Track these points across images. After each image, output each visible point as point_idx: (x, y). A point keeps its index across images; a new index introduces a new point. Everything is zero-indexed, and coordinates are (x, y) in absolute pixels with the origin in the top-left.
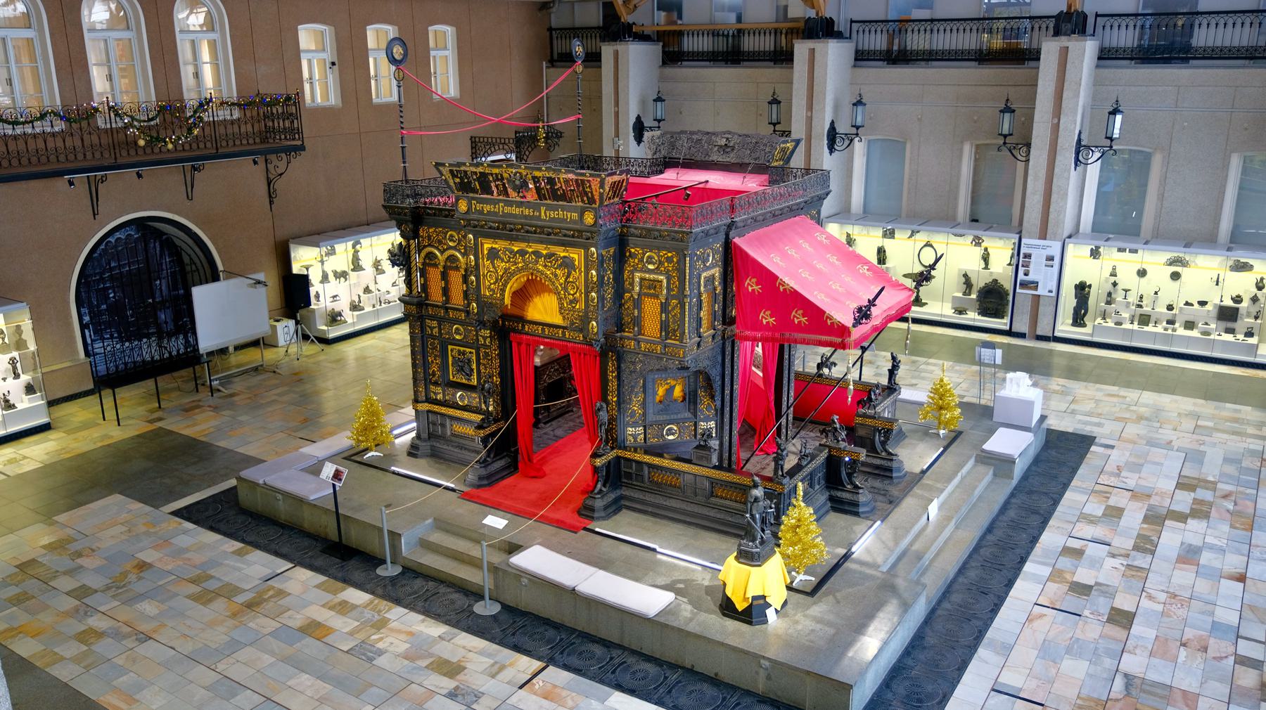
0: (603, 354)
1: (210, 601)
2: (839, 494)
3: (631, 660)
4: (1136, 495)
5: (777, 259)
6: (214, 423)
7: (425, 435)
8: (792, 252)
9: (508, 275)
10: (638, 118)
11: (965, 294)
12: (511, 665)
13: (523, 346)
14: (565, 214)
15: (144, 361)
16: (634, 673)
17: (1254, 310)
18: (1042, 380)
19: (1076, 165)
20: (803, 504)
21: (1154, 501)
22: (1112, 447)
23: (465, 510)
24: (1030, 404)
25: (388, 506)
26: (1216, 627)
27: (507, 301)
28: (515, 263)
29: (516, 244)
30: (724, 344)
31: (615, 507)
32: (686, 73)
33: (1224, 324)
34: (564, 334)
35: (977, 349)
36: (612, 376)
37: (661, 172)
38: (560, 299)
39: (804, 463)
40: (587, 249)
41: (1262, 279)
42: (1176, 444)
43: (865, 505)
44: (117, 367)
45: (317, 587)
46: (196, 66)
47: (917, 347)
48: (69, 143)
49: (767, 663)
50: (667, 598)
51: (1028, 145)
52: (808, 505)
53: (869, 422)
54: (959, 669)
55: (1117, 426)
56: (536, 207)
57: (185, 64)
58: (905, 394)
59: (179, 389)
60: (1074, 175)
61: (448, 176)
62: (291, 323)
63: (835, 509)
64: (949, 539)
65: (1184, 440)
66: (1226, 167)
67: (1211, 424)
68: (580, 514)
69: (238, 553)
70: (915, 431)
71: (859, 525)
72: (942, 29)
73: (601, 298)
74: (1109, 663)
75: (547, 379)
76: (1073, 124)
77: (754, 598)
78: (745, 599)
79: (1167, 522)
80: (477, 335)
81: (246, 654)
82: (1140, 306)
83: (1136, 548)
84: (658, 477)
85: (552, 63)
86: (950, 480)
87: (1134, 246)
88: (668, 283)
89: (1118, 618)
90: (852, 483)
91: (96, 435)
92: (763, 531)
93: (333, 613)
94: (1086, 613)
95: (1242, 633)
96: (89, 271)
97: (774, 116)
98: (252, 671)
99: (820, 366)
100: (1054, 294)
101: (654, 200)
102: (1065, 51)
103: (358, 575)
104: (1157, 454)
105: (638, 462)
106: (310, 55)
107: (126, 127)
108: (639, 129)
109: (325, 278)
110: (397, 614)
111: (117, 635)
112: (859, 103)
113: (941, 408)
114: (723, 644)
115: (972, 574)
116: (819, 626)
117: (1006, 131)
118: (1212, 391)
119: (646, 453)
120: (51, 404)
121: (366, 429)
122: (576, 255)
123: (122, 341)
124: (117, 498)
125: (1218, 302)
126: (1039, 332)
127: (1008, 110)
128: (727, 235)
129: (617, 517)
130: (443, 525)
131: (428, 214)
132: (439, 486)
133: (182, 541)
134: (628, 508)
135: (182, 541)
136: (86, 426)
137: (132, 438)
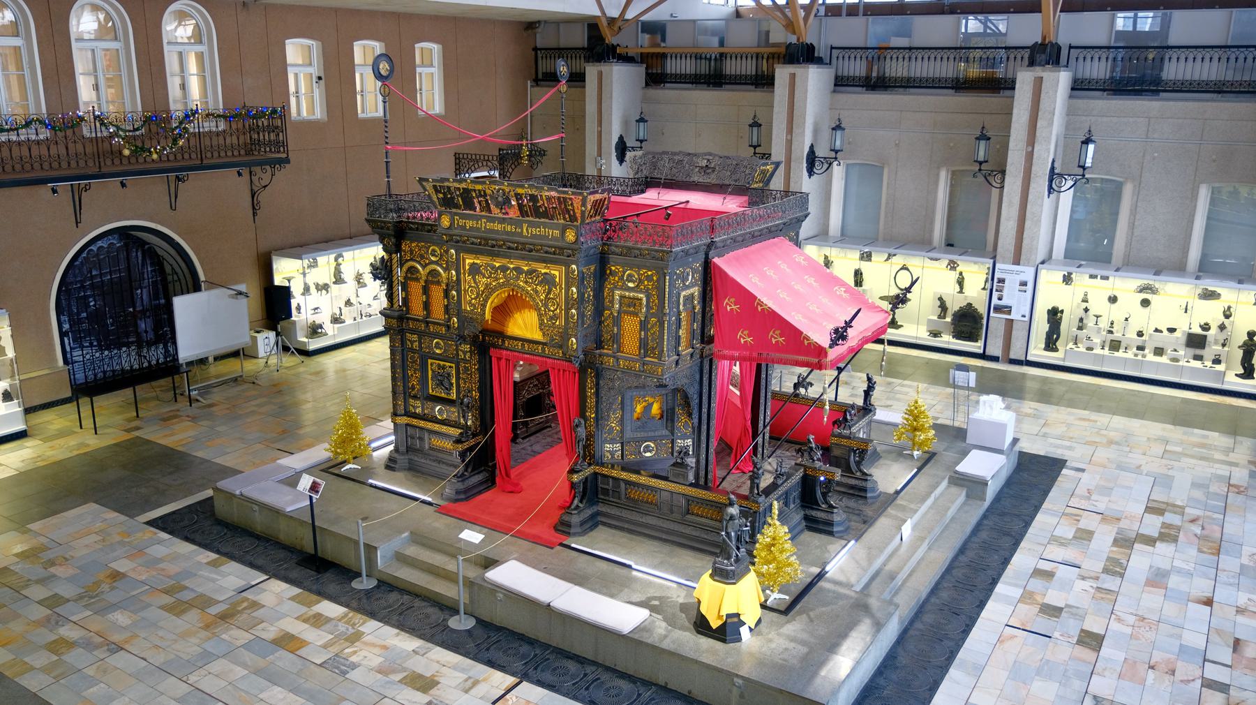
0: (583, 370)
1: (183, 612)
2: (814, 513)
3: (605, 677)
4: (1105, 518)
5: (755, 280)
6: (192, 433)
7: (403, 449)
8: (770, 273)
9: (489, 290)
10: (621, 138)
11: (940, 317)
12: (484, 680)
13: (503, 362)
14: (547, 232)
15: (122, 370)
16: (608, 690)
17: (1221, 338)
18: (1015, 403)
19: (1049, 193)
20: (778, 523)
21: (1124, 524)
22: (1083, 470)
23: (441, 523)
24: (1002, 427)
25: (364, 519)
26: (1183, 650)
27: (488, 316)
28: (497, 279)
29: (498, 259)
30: (702, 363)
31: (592, 523)
32: (667, 93)
33: (1192, 351)
34: (543, 350)
35: (952, 371)
36: (590, 392)
37: (643, 192)
38: (540, 315)
39: (780, 482)
40: (568, 266)
41: (1229, 308)
42: (1145, 469)
43: (840, 524)
44: (95, 375)
45: (292, 599)
46: (183, 78)
47: (892, 369)
48: (53, 151)
49: (741, 682)
50: (643, 614)
51: (1003, 172)
52: (783, 524)
53: (844, 442)
54: (964, 631)
55: (1089, 450)
56: (518, 224)
57: (172, 75)
58: (880, 415)
59: (157, 398)
60: (1047, 202)
61: (432, 191)
62: (272, 335)
63: (810, 529)
64: (922, 559)
65: (1156, 466)
66: (1194, 197)
67: (1179, 449)
68: (555, 528)
69: (213, 564)
70: (890, 452)
71: (834, 545)
72: (920, 57)
73: (581, 315)
74: (1078, 685)
75: (526, 395)
76: (1047, 153)
77: (728, 616)
78: (720, 617)
79: (1136, 546)
80: (457, 350)
81: (217, 666)
82: (1111, 332)
83: (1106, 571)
84: (635, 494)
85: (537, 81)
86: (924, 500)
87: (1105, 273)
89: (1087, 640)
90: (827, 502)
91: (72, 443)
92: (738, 549)
93: (307, 626)
94: (1056, 635)
95: (1209, 656)
96: (70, 279)
97: (755, 139)
98: (224, 684)
99: (796, 386)
100: (1027, 319)
101: (636, 219)
102: (1039, 82)
103: (332, 588)
104: (1127, 478)
105: (613, 478)
106: (296, 70)
107: (111, 136)
108: (622, 149)
109: (307, 290)
110: (372, 629)
111: (89, 646)
112: (838, 127)
113: (915, 429)
114: (697, 662)
115: (944, 595)
116: (792, 645)
117: (981, 158)
118: (1182, 417)
119: (623, 469)
120: (28, 411)
121: (344, 442)
122: (557, 272)
123: (101, 349)
124: (93, 507)
125: (1187, 329)
126: (1012, 356)
127: (983, 137)
128: (707, 255)
129: (594, 533)
130: (419, 539)
131: (411, 229)
132: (416, 499)
133: (158, 551)
134: (604, 524)
135: (158, 551)
136: (62, 434)
137: (108, 447)
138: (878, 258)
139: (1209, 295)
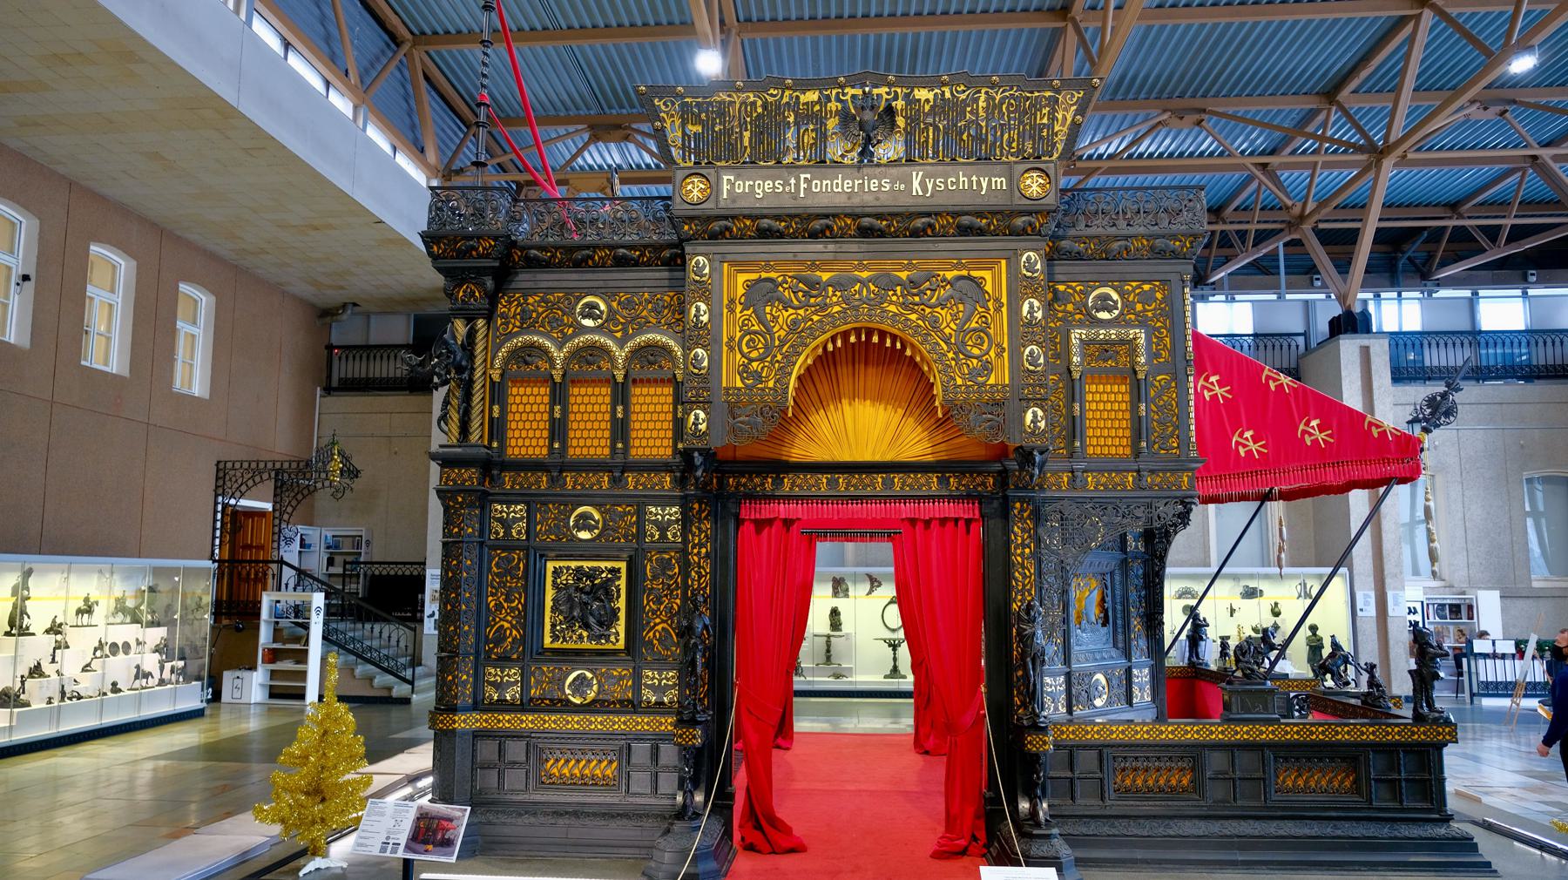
80: (640, 523)
85: (328, 390)
88: (1148, 339)
138: (858, 591)
139: (1250, 593)
